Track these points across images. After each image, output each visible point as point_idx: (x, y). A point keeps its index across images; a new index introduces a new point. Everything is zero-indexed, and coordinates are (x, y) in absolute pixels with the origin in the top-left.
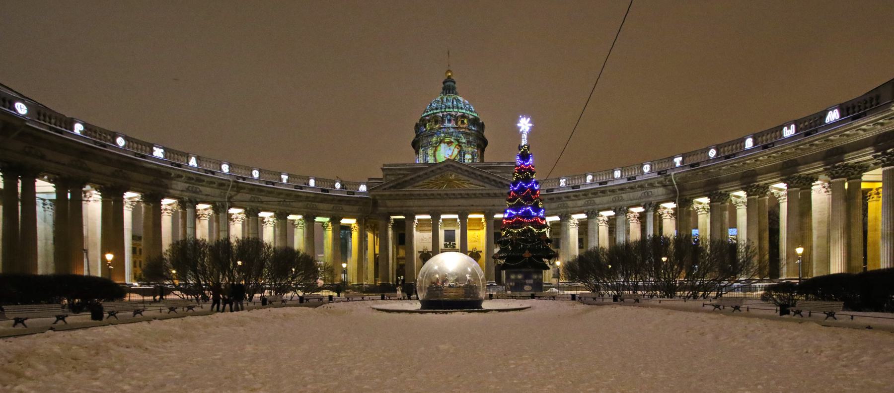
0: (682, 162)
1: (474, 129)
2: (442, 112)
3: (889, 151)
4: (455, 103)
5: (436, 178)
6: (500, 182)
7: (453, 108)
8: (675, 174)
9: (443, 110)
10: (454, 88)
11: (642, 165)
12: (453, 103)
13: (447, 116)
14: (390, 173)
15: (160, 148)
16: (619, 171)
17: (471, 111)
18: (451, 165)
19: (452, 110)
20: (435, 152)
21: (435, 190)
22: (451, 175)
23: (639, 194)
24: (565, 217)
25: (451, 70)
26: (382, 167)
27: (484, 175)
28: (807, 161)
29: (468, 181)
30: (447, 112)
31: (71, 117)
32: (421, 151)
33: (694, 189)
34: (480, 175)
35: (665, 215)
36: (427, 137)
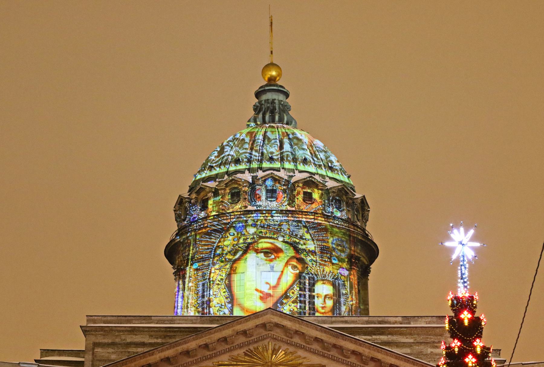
1: (338, 214)
2: (250, 170)
4: (287, 147)
5: (233, 359)
7: (282, 160)
9: (255, 165)
10: (285, 109)
12: (281, 147)
17: (331, 169)
18: (277, 325)
19: (277, 165)
20: (229, 276)
22: (275, 351)
26: (84, 324)
32: (190, 271)
36: (208, 234)
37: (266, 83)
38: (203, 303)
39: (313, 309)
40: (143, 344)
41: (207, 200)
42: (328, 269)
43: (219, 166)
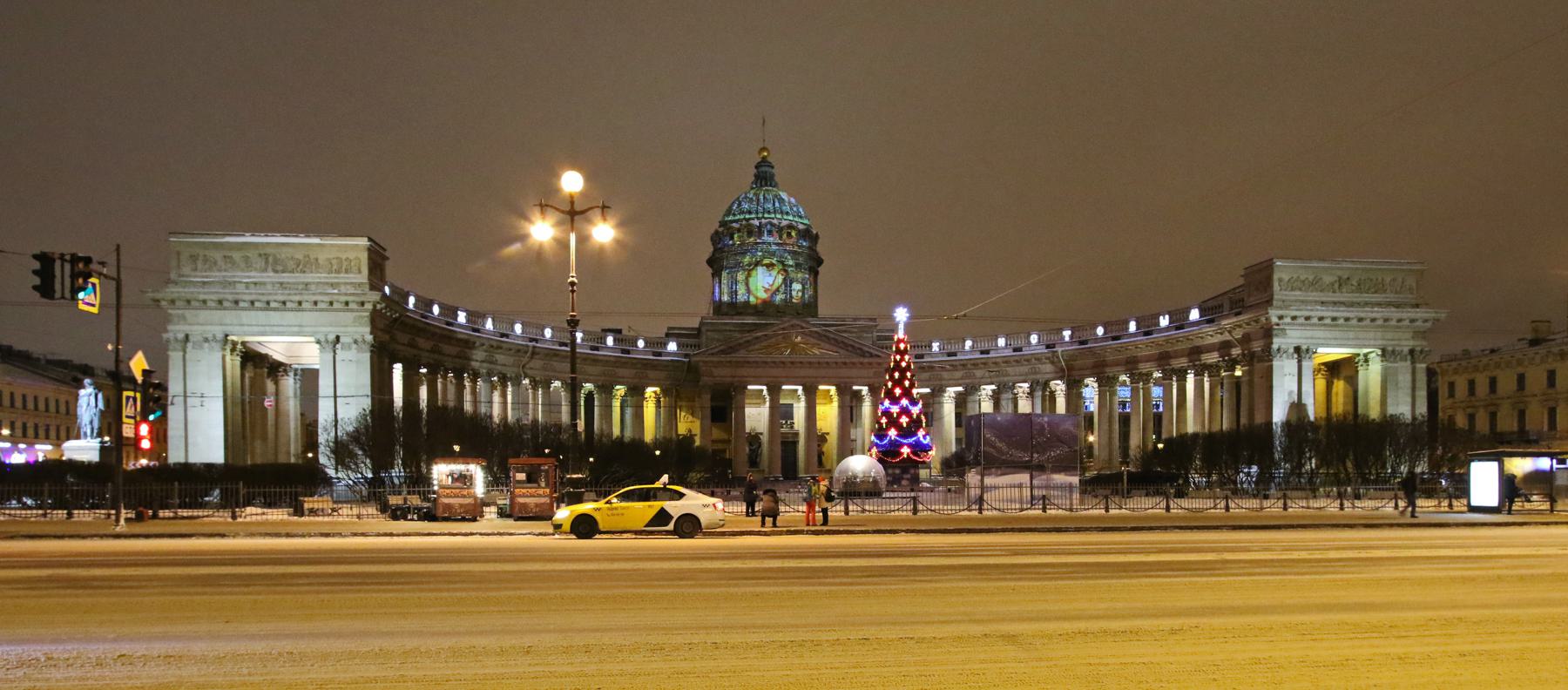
0: (1071, 337)
1: (804, 244)
2: (758, 218)
3: (1226, 358)
4: (777, 205)
6: (859, 349)
8: (1062, 351)
9: (760, 215)
10: (772, 176)
11: (1029, 335)
12: (774, 205)
13: (766, 226)
14: (712, 328)
16: (1004, 339)
17: (801, 217)
19: (773, 216)
20: (747, 278)
21: (776, 357)
22: (796, 338)
23: (1025, 369)
24: (938, 392)
25: (769, 149)
28: (1177, 355)
29: (819, 345)
30: (766, 218)
32: (724, 274)
33: (1083, 369)
34: (833, 339)
35: (1059, 392)
37: (760, 160)
38: (732, 292)
39: (791, 297)
40: (730, 331)
41: (734, 234)
42: (799, 275)
43: (739, 214)
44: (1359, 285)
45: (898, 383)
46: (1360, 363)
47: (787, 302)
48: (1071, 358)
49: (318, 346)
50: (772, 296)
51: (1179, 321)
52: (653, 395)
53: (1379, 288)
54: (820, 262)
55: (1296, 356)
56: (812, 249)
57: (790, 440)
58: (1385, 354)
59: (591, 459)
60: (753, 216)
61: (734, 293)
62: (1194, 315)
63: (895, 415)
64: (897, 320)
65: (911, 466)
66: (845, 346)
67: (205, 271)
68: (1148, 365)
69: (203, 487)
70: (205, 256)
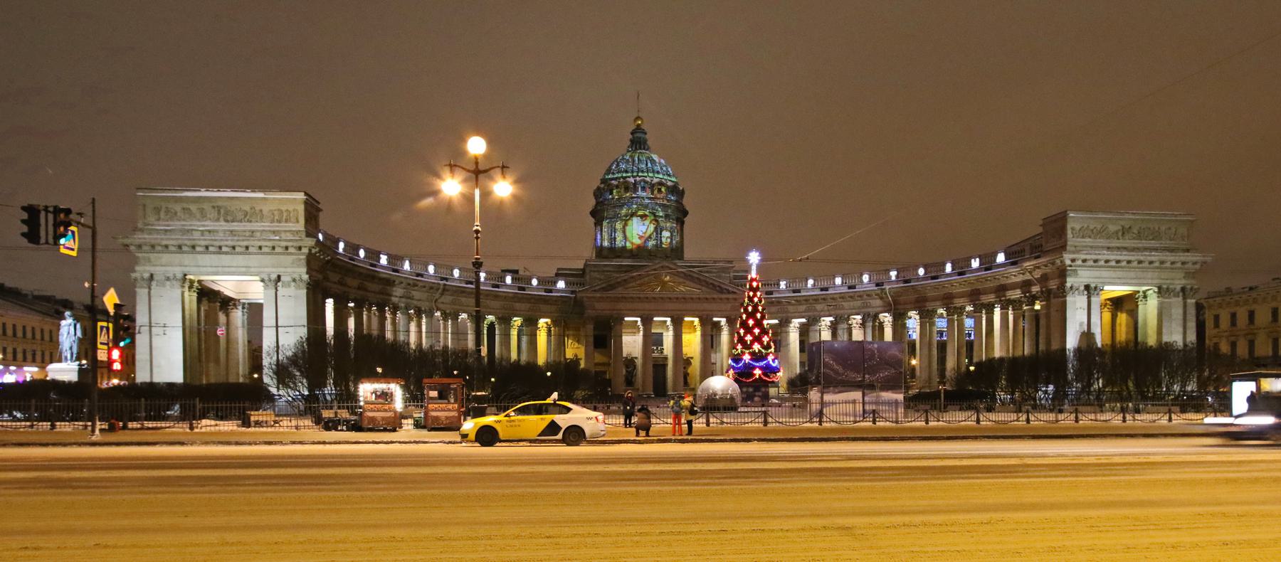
0: (897, 276)
1: (673, 198)
2: (633, 177)
4: (649, 165)
7: (647, 172)
8: (890, 289)
9: (635, 174)
10: (645, 141)
11: (862, 275)
12: (647, 165)
15: (385, 255)
16: (840, 278)
17: (669, 175)
20: (624, 227)
21: (649, 294)
22: (666, 277)
23: (858, 303)
24: (785, 323)
27: (702, 278)
28: (985, 292)
29: (684, 283)
31: (358, 243)
32: (605, 223)
35: (886, 323)
36: (614, 207)
38: (611, 239)
40: (610, 271)
41: (613, 190)
42: (668, 225)
43: (618, 173)
44: (1139, 233)
45: (751, 315)
46: (1140, 299)
47: (658, 246)
48: (897, 295)
49: (262, 284)
50: (645, 242)
51: (988, 263)
52: (545, 325)
53: (1156, 236)
54: (685, 213)
55: (1086, 293)
56: (679, 202)
57: (661, 363)
58: (1161, 291)
59: (493, 380)
60: (629, 174)
61: (613, 240)
62: (1001, 258)
63: (749, 343)
64: (751, 262)
65: (762, 385)
66: (707, 284)
67: (167, 221)
68: (962, 300)
69: (43, 404)
70: (167, 208)
